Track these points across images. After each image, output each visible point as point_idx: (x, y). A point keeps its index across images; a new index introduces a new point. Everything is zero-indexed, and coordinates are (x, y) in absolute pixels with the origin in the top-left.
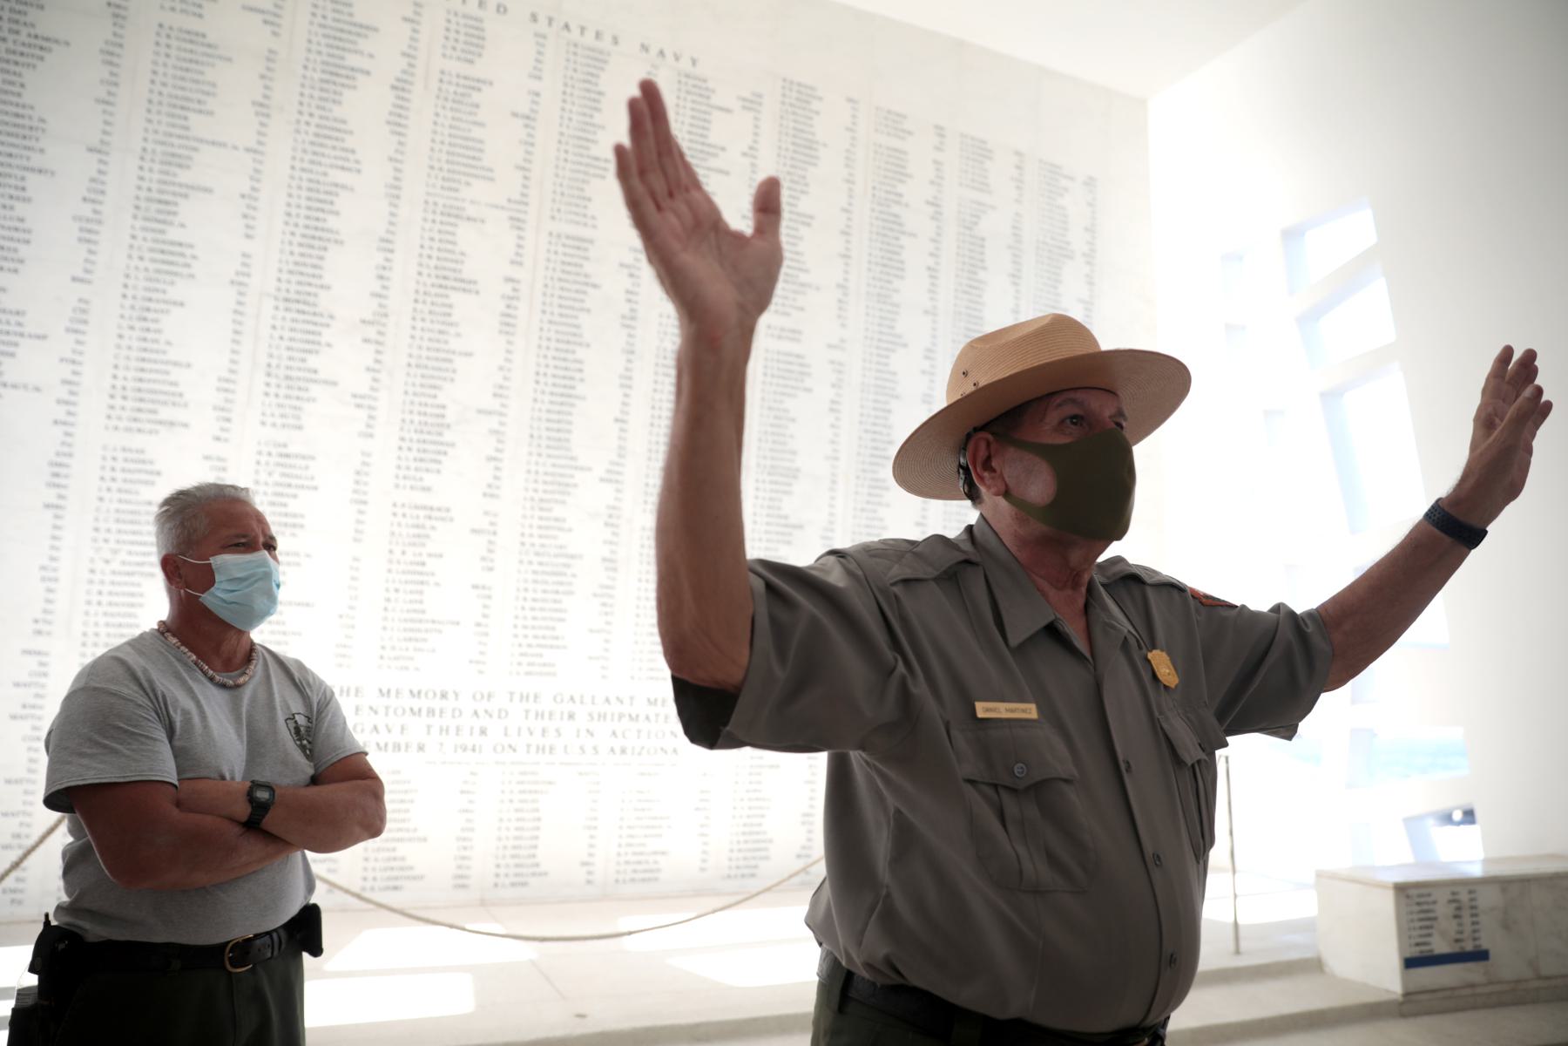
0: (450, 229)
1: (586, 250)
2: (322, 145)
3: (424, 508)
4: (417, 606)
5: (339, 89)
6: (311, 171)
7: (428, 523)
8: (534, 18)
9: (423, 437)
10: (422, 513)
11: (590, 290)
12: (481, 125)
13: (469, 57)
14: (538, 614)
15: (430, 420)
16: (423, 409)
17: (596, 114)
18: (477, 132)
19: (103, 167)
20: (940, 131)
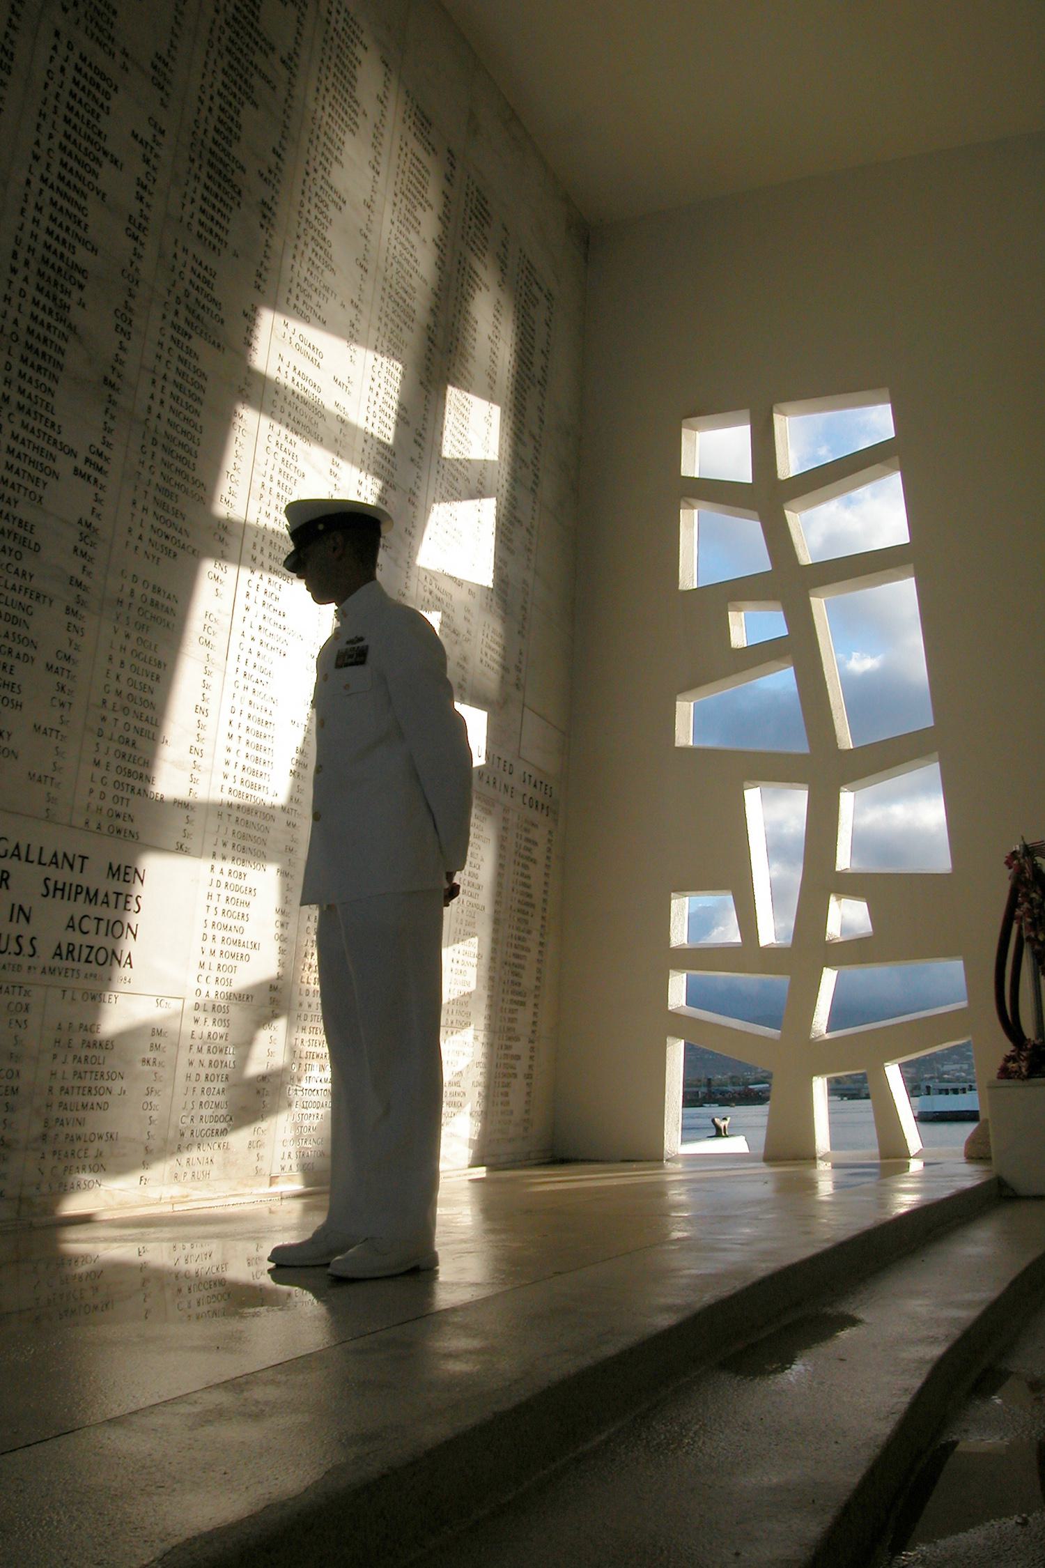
11: (106, 161)
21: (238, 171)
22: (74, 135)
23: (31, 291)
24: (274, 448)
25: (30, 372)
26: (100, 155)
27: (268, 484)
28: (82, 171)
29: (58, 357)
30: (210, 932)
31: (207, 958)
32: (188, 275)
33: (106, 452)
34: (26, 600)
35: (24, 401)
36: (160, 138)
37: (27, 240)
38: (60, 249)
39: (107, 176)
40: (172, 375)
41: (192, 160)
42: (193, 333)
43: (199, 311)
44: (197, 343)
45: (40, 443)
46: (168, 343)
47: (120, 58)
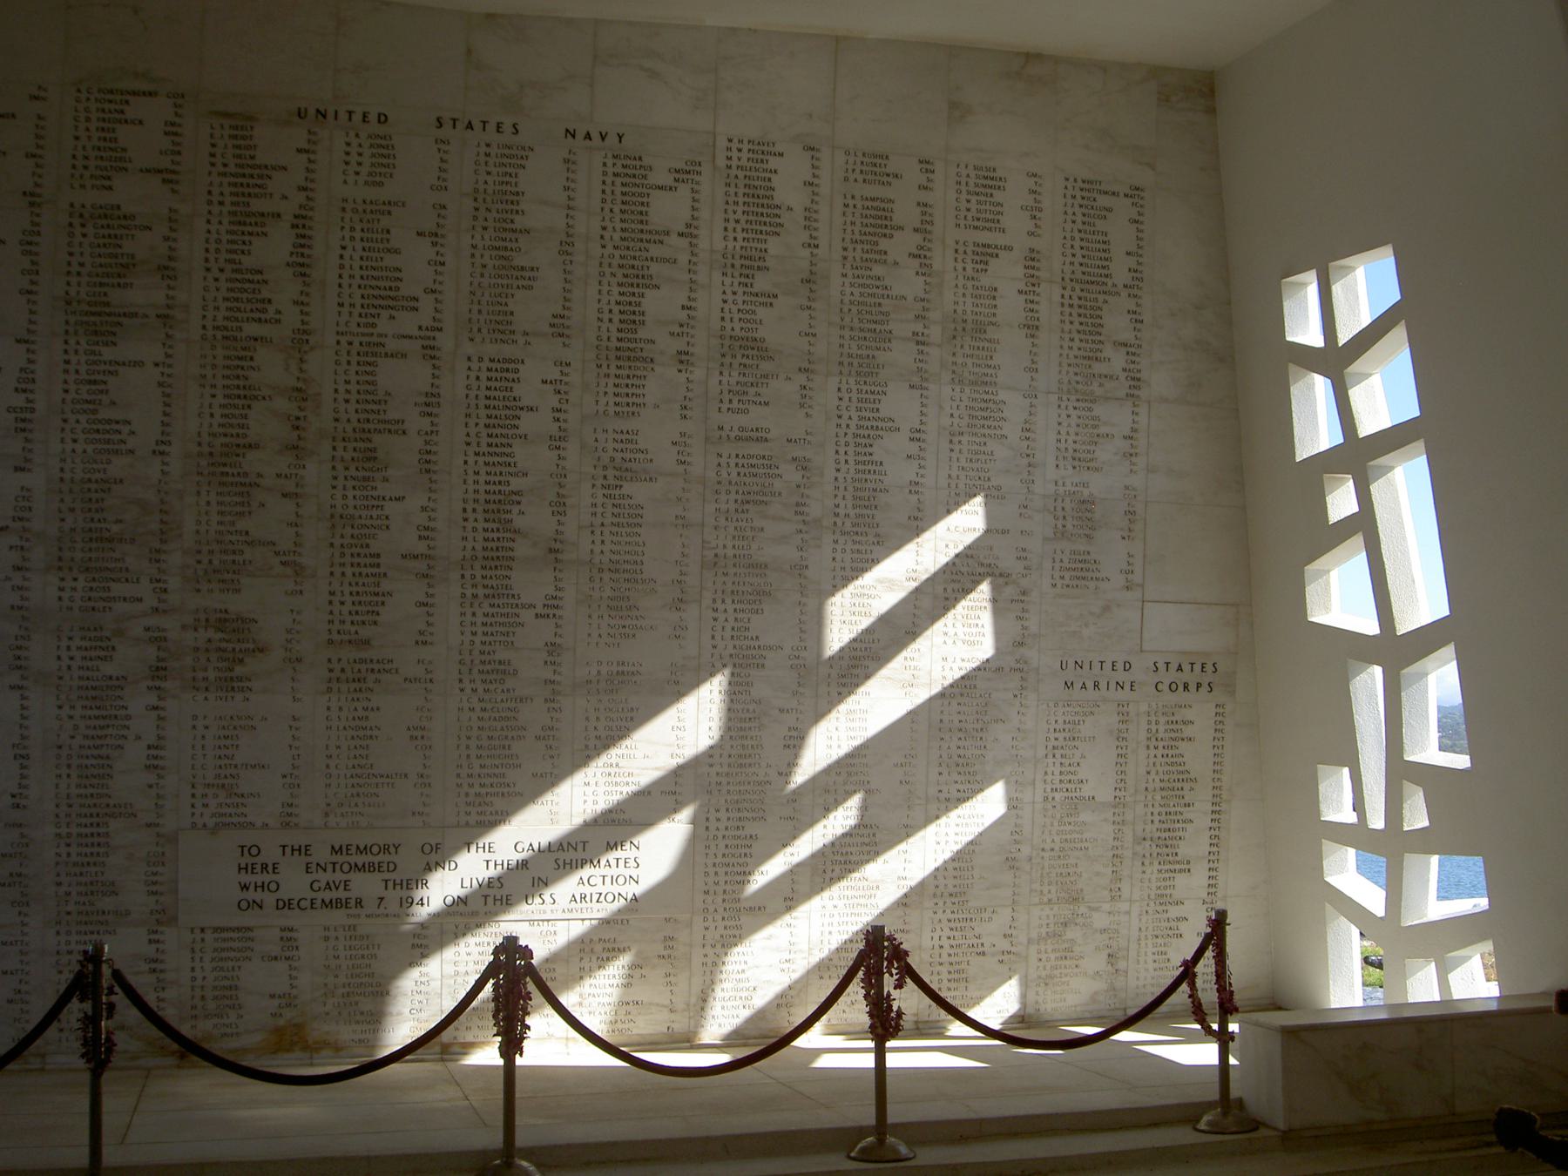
0: (368, 369)
1: (517, 371)
2: (236, 300)
3: (363, 661)
4: (364, 762)
5: (246, 238)
6: (226, 328)
7: (371, 677)
8: (440, 123)
9: (354, 589)
10: (363, 667)
11: (523, 414)
12: (397, 251)
13: (378, 179)
14: (488, 762)
15: (364, 571)
16: (356, 560)
17: (517, 218)
18: (389, 260)
19: (31, 356)
20: (926, 164)
21: (649, 346)
22: (494, 412)
23: (481, 525)
24: (722, 521)
25: (488, 573)
26: (518, 412)
27: (720, 551)
28: (504, 431)
29: (511, 554)
30: (711, 870)
31: (712, 888)
32: (611, 445)
33: (559, 594)
34: (513, 705)
35: (487, 591)
36: (566, 370)
37: (471, 496)
38: (497, 488)
39: (527, 423)
40: (606, 522)
41: (599, 366)
42: (625, 484)
43: (629, 465)
44: (628, 488)
45: (505, 611)
46: (600, 500)
47: (521, 340)
